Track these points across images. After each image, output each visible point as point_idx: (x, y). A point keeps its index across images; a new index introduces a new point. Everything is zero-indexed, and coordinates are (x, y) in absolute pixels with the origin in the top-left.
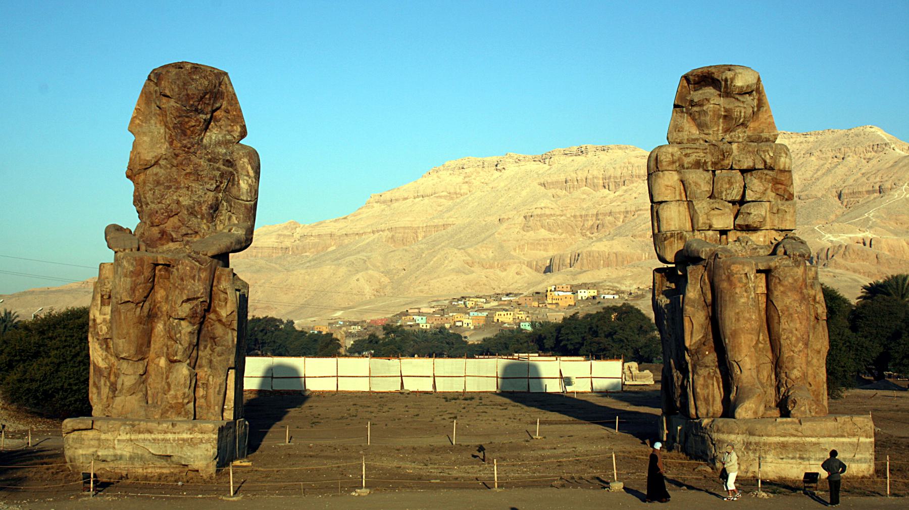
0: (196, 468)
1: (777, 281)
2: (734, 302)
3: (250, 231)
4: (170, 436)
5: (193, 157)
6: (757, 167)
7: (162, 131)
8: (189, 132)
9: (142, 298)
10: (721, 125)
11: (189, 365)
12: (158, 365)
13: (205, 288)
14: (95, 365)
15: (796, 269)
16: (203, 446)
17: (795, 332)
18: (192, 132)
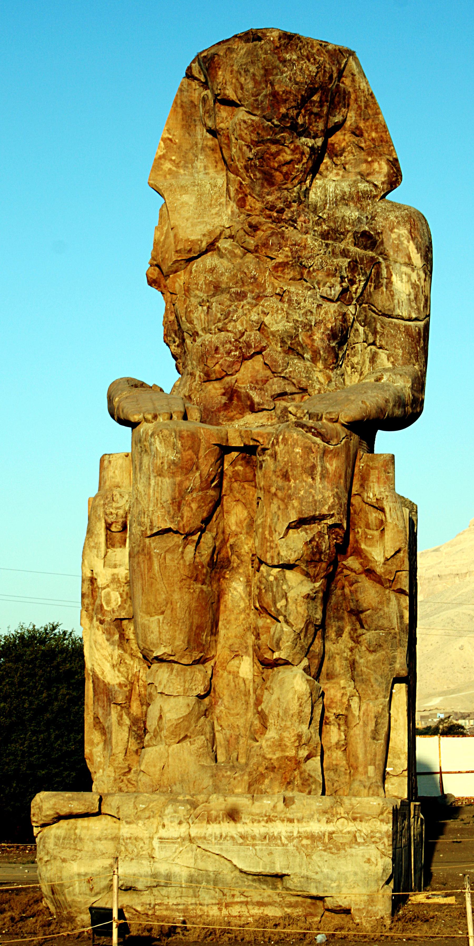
0: (344, 903)
3: (419, 384)
4: (280, 828)
5: (289, 231)
7: (221, 181)
8: (278, 176)
9: (197, 523)
11: (307, 670)
12: (236, 675)
13: (337, 496)
14: (96, 680)
16: (358, 851)
18: (286, 176)
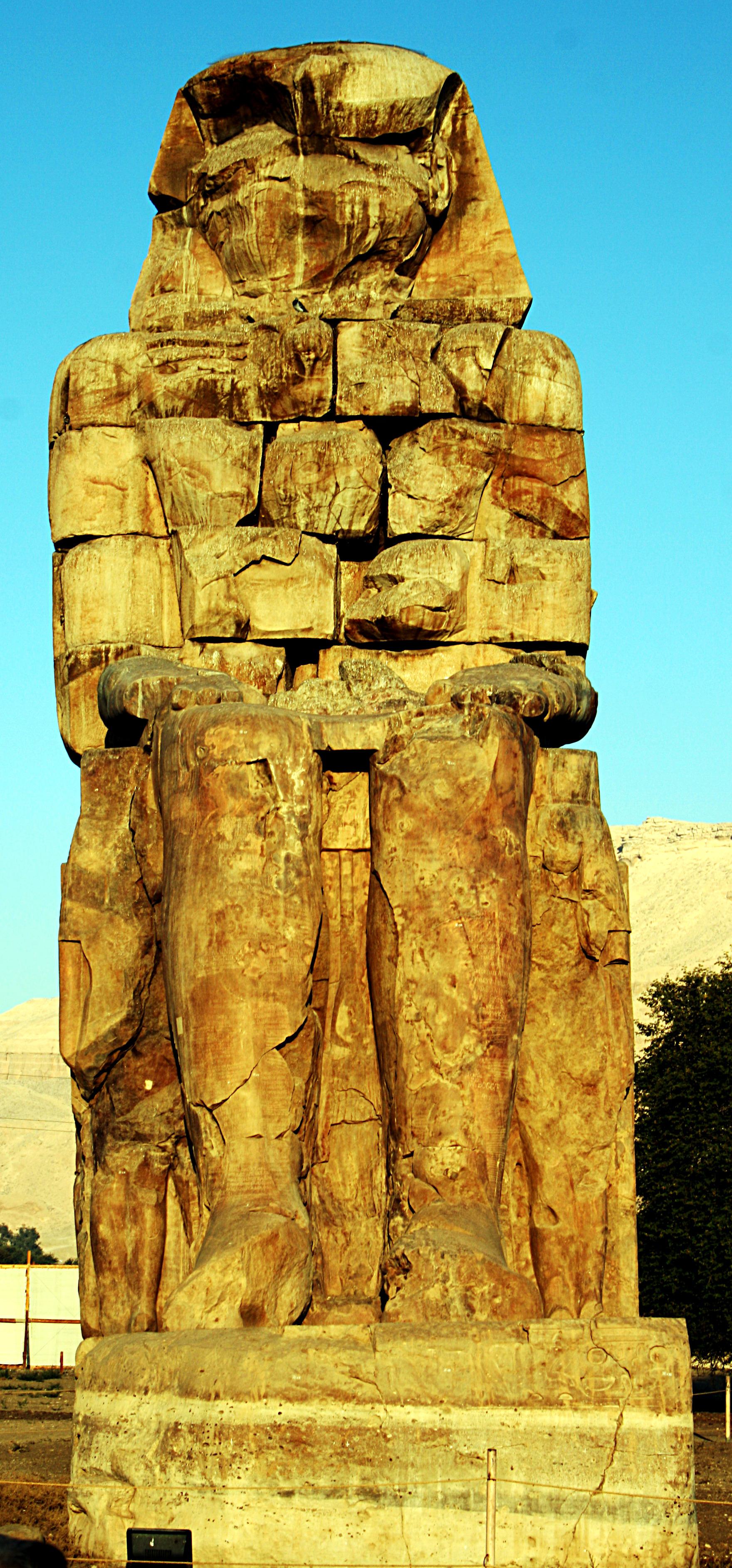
1: (395, 793)
2: (210, 871)
6: (425, 406)
10: (302, 258)
15: (470, 750)
17: (447, 990)
